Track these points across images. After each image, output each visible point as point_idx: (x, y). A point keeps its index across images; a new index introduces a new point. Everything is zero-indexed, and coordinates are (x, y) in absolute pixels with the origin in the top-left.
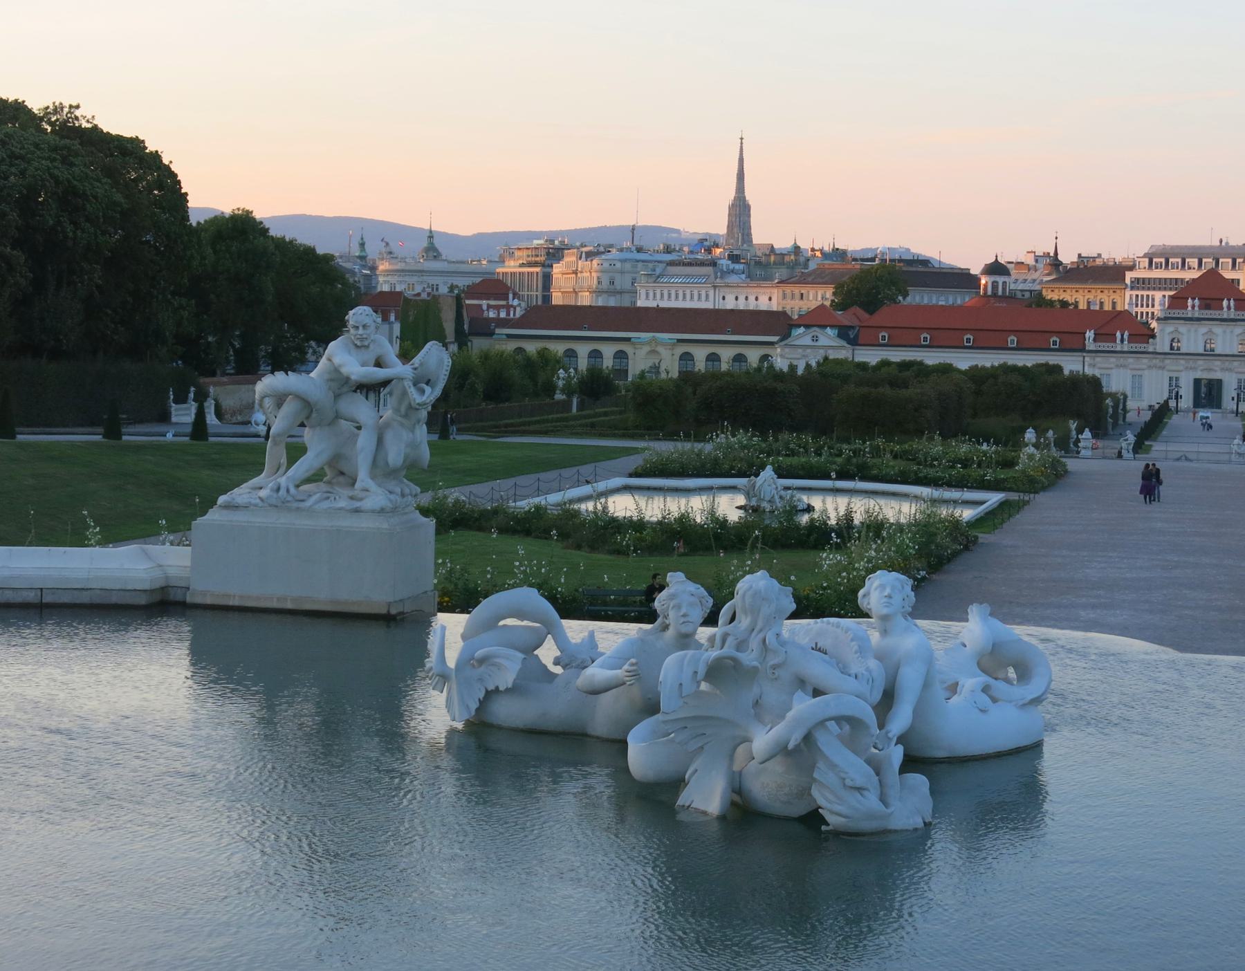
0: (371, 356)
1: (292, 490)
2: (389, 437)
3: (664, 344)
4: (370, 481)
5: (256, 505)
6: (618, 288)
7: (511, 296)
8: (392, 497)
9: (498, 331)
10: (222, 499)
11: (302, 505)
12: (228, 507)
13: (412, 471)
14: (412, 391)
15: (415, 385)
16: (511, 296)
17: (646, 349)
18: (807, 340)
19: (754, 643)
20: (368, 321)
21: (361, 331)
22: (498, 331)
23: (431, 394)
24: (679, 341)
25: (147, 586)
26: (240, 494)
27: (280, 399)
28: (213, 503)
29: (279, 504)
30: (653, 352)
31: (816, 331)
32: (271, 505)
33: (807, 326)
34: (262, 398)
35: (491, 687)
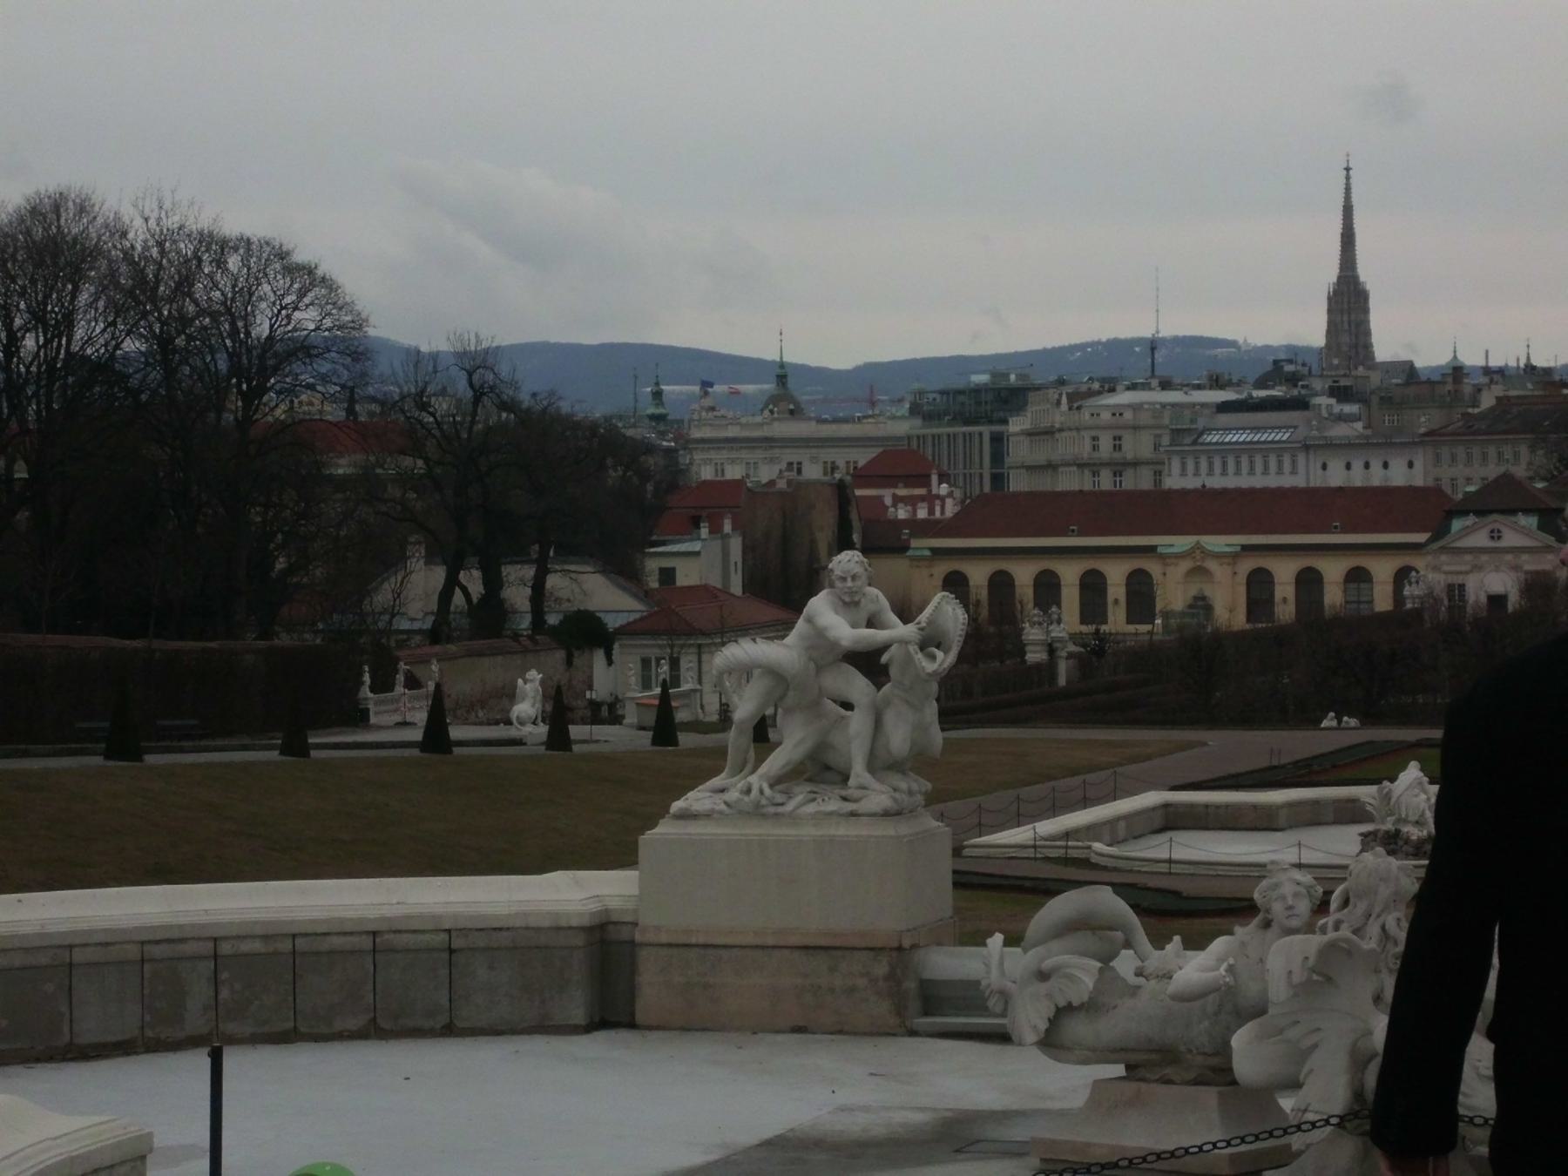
0: (863, 616)
1: (767, 791)
2: (889, 718)
3: (1218, 556)
4: (868, 776)
5: (721, 812)
6: (1130, 456)
7: (934, 478)
8: (897, 795)
9: (914, 543)
10: (677, 806)
11: (780, 809)
12: (686, 816)
13: (919, 762)
14: (919, 657)
15: (922, 649)
16: (934, 478)
17: (1185, 565)
18: (1480, 539)
19: (1374, 929)
20: (858, 569)
21: (849, 584)
22: (914, 543)
23: (944, 660)
24: (1245, 548)
25: (586, 922)
26: (697, 799)
27: (746, 671)
28: (664, 811)
29: (757, 812)
30: (1199, 571)
31: (1496, 521)
32: (740, 812)
33: (1480, 513)
34: (721, 674)
35: (1062, 1003)
